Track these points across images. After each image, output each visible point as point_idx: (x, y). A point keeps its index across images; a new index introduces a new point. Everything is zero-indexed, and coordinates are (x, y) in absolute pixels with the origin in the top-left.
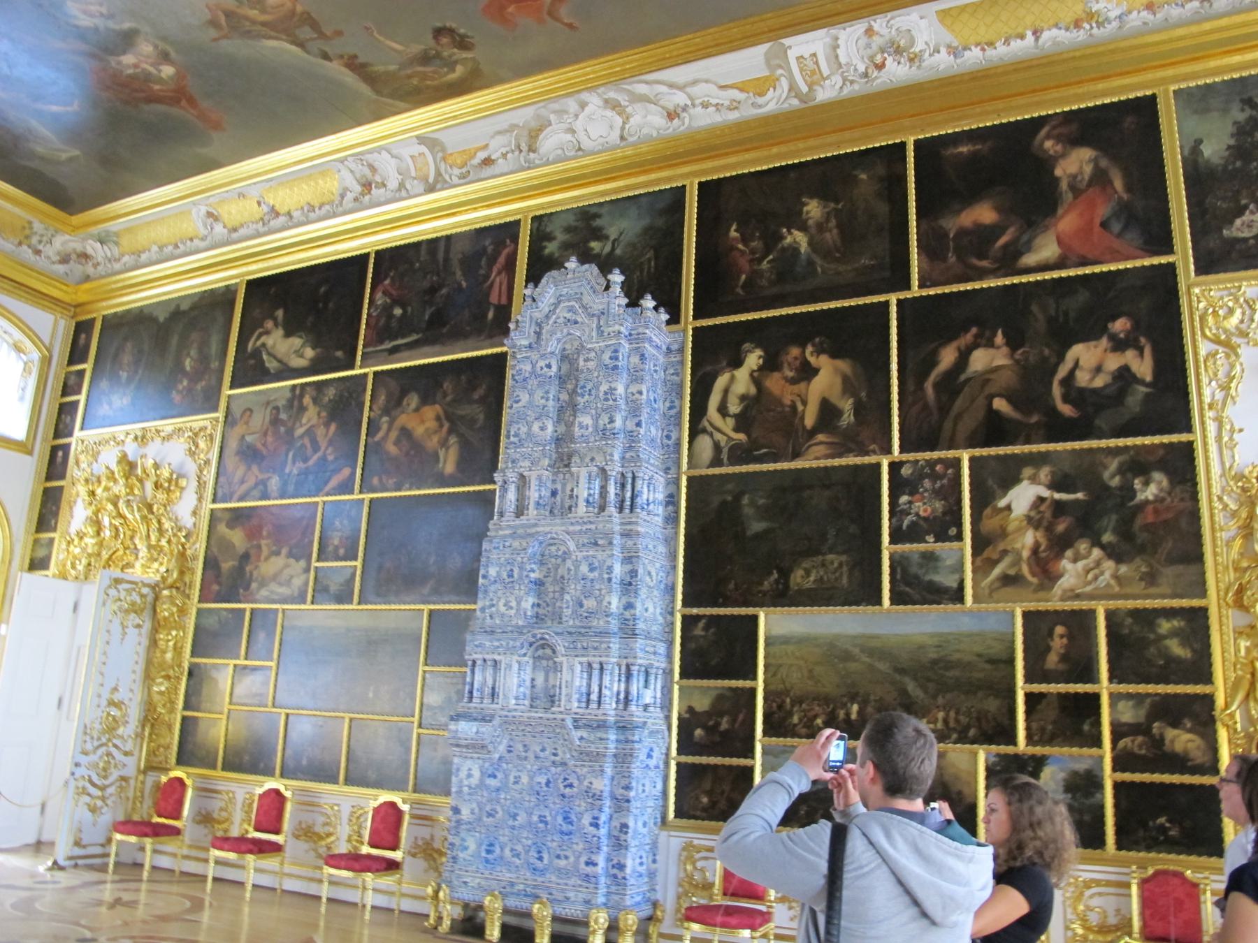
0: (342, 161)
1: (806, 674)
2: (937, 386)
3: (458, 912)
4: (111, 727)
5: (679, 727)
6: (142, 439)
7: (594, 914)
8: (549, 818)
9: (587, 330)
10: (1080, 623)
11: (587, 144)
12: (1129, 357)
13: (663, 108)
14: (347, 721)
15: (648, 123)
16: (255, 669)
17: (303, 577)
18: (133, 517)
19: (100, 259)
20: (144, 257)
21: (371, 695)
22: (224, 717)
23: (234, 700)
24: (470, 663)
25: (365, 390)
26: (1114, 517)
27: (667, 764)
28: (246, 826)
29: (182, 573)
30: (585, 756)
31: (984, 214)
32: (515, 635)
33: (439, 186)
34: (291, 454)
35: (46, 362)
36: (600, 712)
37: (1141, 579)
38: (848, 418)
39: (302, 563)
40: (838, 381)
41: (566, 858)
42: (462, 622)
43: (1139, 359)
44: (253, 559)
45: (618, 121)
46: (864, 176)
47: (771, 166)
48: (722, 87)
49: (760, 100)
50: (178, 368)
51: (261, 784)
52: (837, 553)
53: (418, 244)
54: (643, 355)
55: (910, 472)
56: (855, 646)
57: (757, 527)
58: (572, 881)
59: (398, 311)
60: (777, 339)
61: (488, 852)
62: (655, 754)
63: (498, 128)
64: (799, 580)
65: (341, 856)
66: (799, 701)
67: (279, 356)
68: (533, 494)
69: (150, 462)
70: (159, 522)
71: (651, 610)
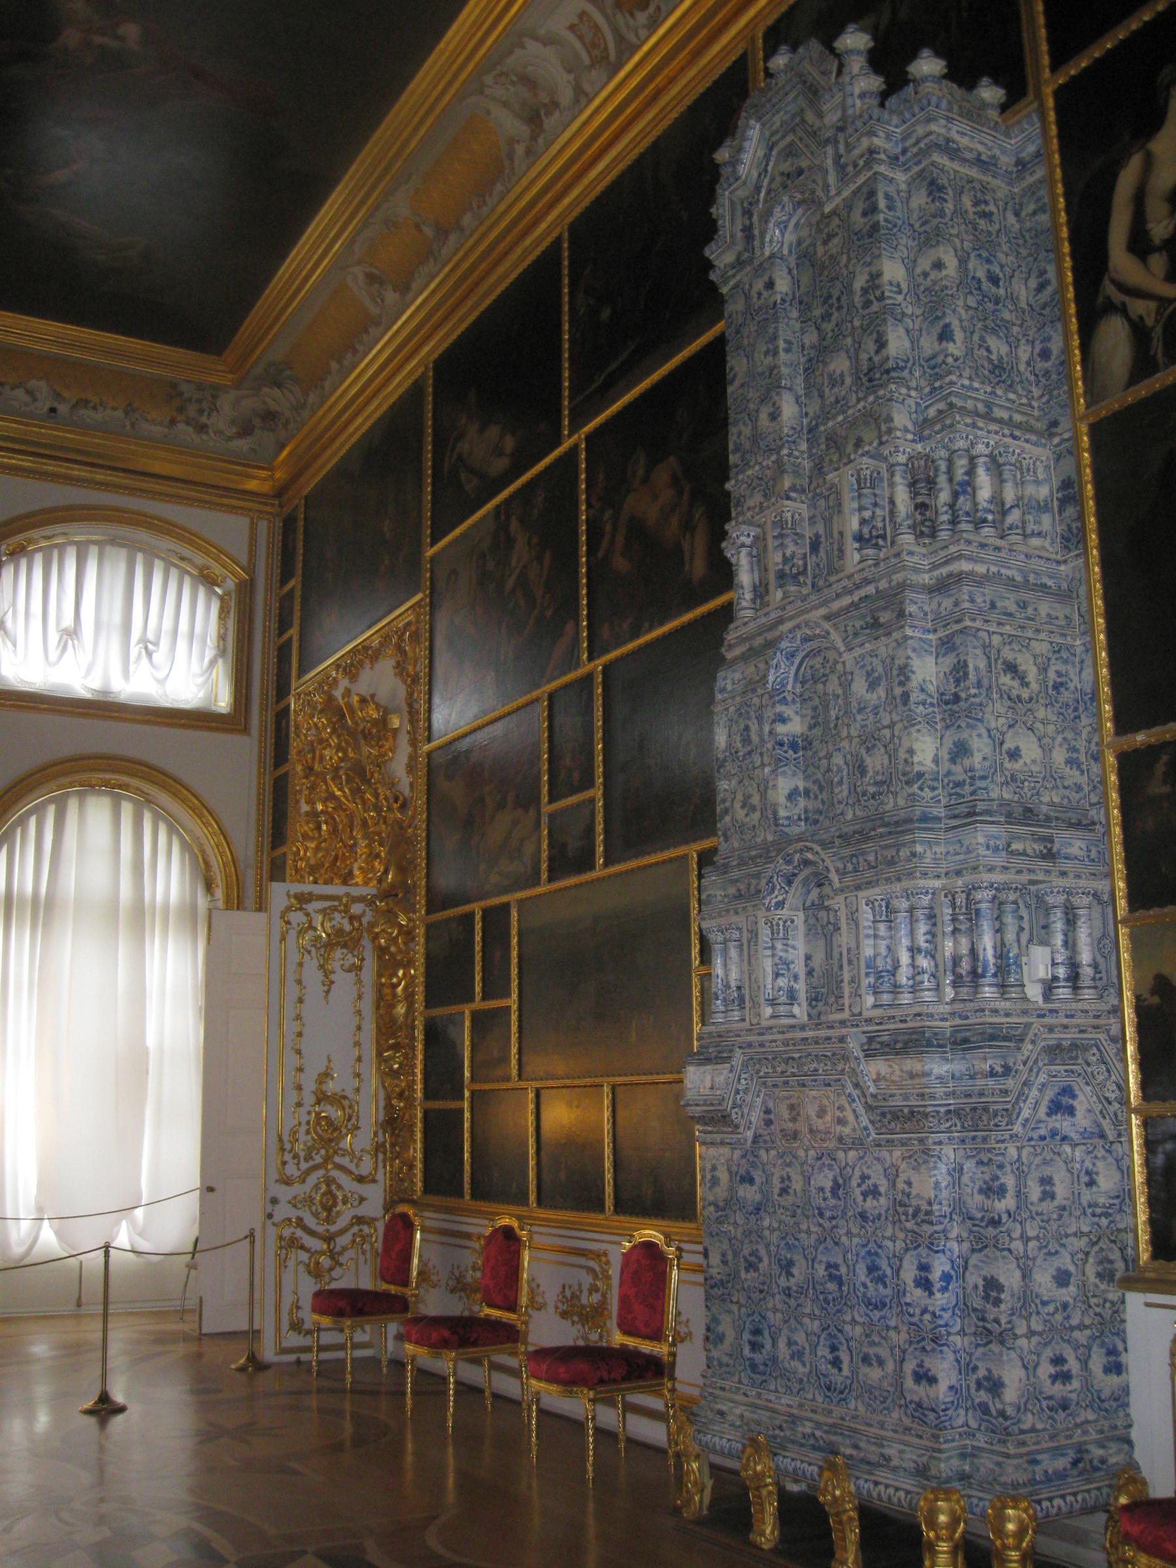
4: (328, 1136)
29: (402, 870)
39: (532, 813)
41: (881, 1362)
51: (491, 1216)
54: (933, 183)
61: (755, 1346)
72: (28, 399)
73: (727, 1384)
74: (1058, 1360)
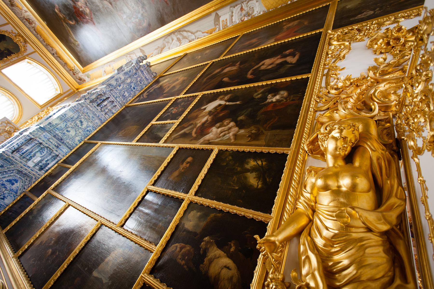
37: (249, 136)
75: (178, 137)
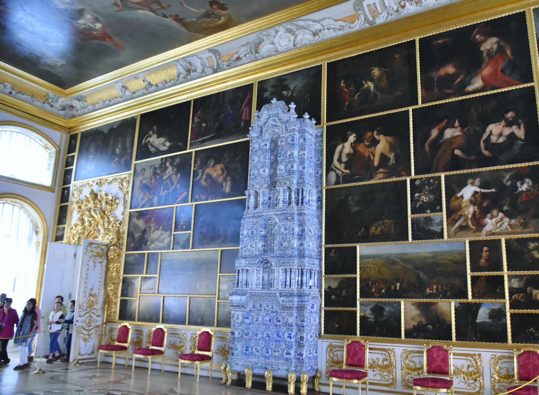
0: (177, 61)
1: (377, 270)
2: (430, 146)
3: (235, 377)
4: (91, 305)
5: (325, 295)
6: (100, 184)
7: (289, 375)
8: (271, 335)
9: (281, 129)
10: (494, 245)
11: (280, 49)
12: (514, 129)
13: (311, 31)
14: (188, 298)
15: (305, 38)
16: (150, 278)
17: (169, 239)
18: (97, 217)
19: (78, 108)
20: (97, 106)
21: (198, 287)
22: (138, 299)
23: (142, 292)
24: (237, 271)
25: (191, 159)
26: (508, 199)
27: (320, 311)
28: (148, 345)
29: (118, 239)
30: (284, 308)
31: (450, 69)
32: (255, 259)
33: (218, 70)
34: (162, 188)
35: (58, 153)
36: (290, 289)
37: (521, 225)
38: (392, 161)
39: (168, 233)
40: (388, 146)
41: (278, 351)
42: (235, 254)
43: (518, 130)
44: (148, 232)
45: (292, 38)
46: (397, 56)
47: (358, 54)
48: (336, 20)
49: (352, 25)
50: (114, 153)
52: (389, 219)
53: (212, 95)
54: (305, 138)
55: (419, 183)
56: (397, 258)
57: (356, 209)
58: (280, 362)
59: (204, 125)
60: (360, 129)
61: (246, 350)
62: (315, 307)
63: (242, 44)
64: (373, 231)
65: (187, 355)
66: (374, 282)
67: (156, 146)
68: (261, 199)
69: (103, 193)
70: (108, 218)
71: (311, 246)
72: (4, 88)
73: (239, 358)
74: (310, 351)
75: (457, 230)
